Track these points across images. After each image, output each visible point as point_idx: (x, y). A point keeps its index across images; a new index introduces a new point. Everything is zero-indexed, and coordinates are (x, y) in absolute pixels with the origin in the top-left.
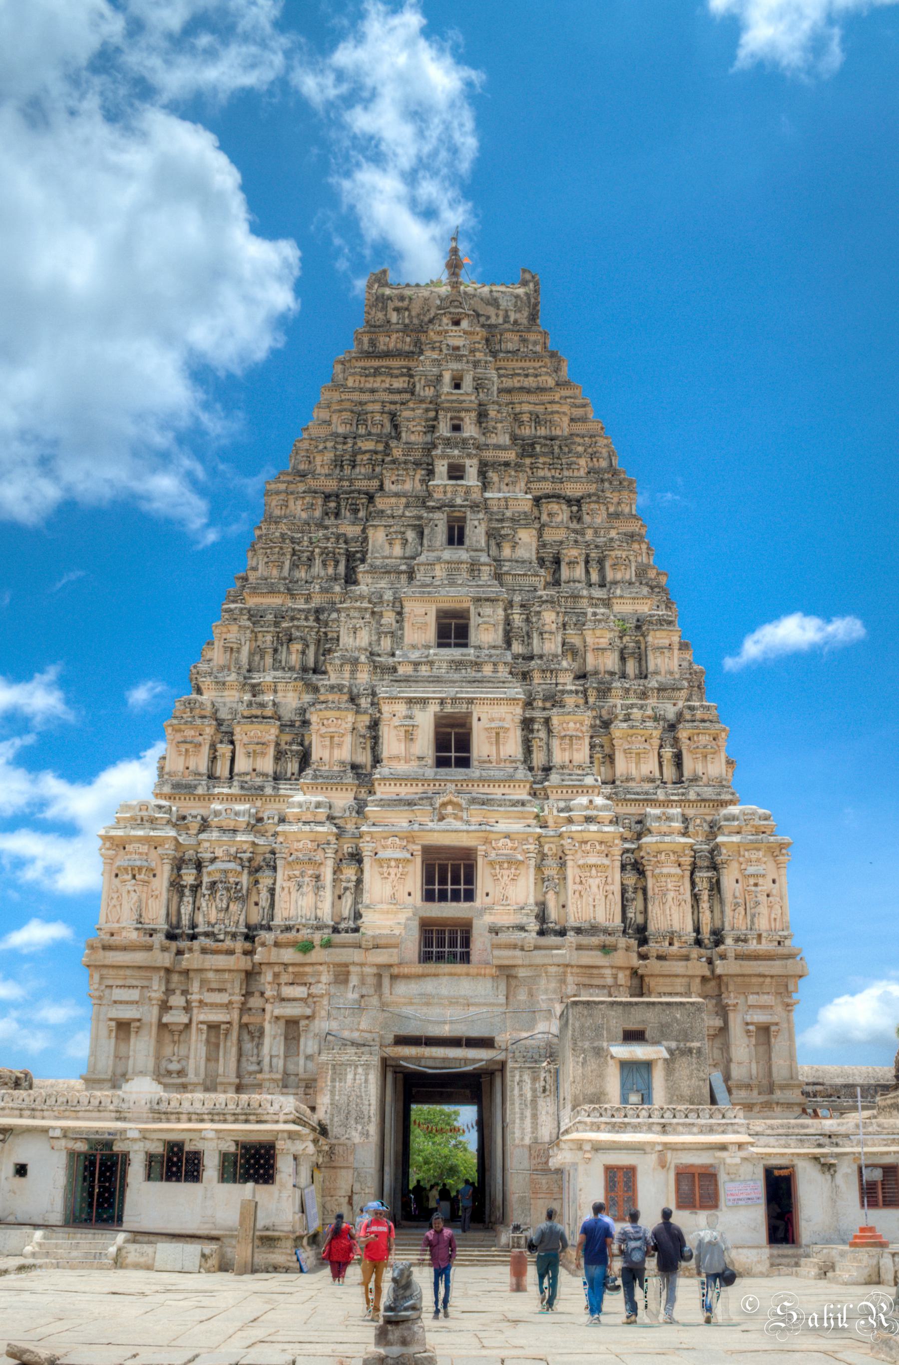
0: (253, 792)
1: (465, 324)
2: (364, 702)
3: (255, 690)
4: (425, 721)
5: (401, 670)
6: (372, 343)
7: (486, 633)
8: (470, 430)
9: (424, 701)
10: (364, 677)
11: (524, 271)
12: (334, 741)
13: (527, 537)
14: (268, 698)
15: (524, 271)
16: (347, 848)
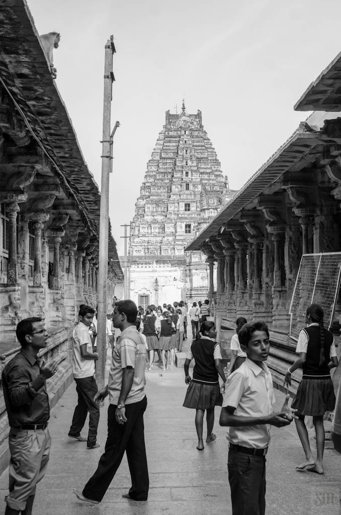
0: (155, 236)
1: (187, 132)
2: (173, 221)
3: (153, 216)
4: (184, 225)
5: (180, 216)
6: (168, 133)
7: (193, 208)
8: (189, 163)
9: (183, 222)
10: (173, 216)
11: (198, 110)
12: (169, 229)
13: (200, 187)
14: (155, 217)
15: (198, 110)
16: (172, 246)
